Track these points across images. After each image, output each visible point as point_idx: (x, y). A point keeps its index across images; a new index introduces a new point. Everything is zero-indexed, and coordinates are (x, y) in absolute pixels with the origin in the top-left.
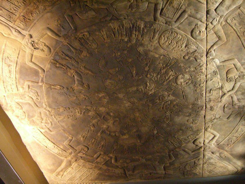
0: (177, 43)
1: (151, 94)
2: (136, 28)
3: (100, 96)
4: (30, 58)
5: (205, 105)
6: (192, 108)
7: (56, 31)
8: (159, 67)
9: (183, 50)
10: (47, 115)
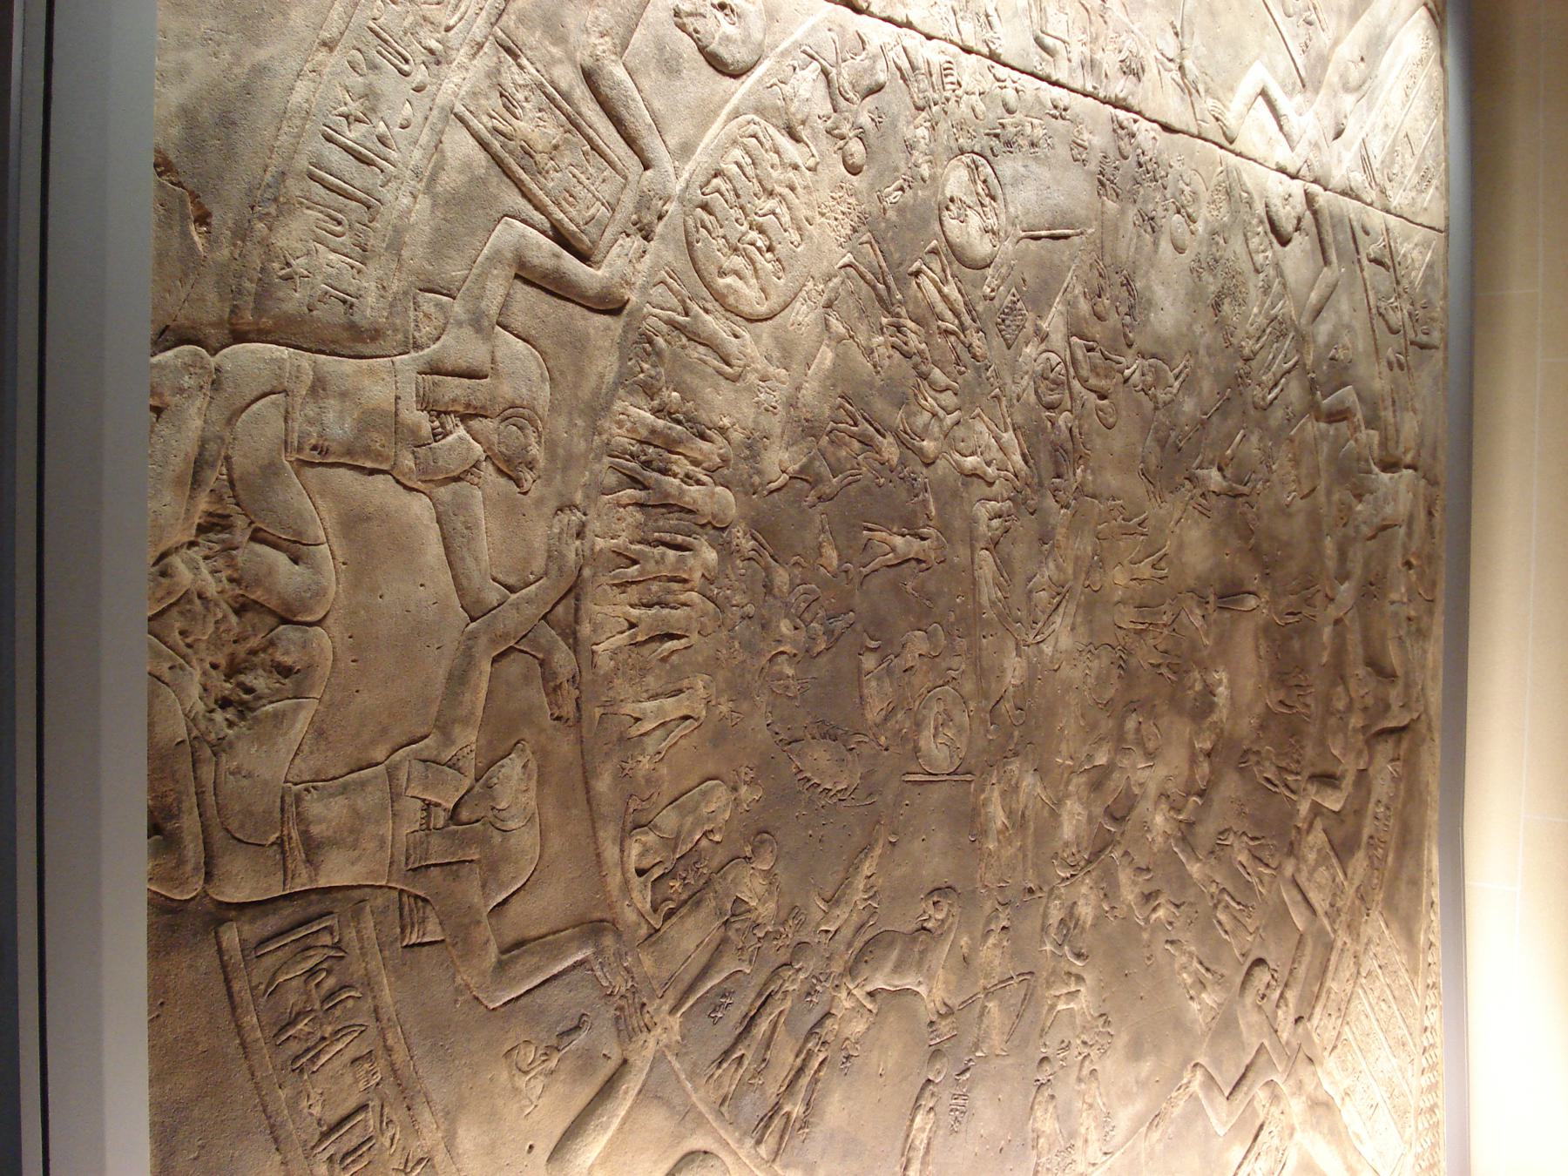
2: (647, 464)
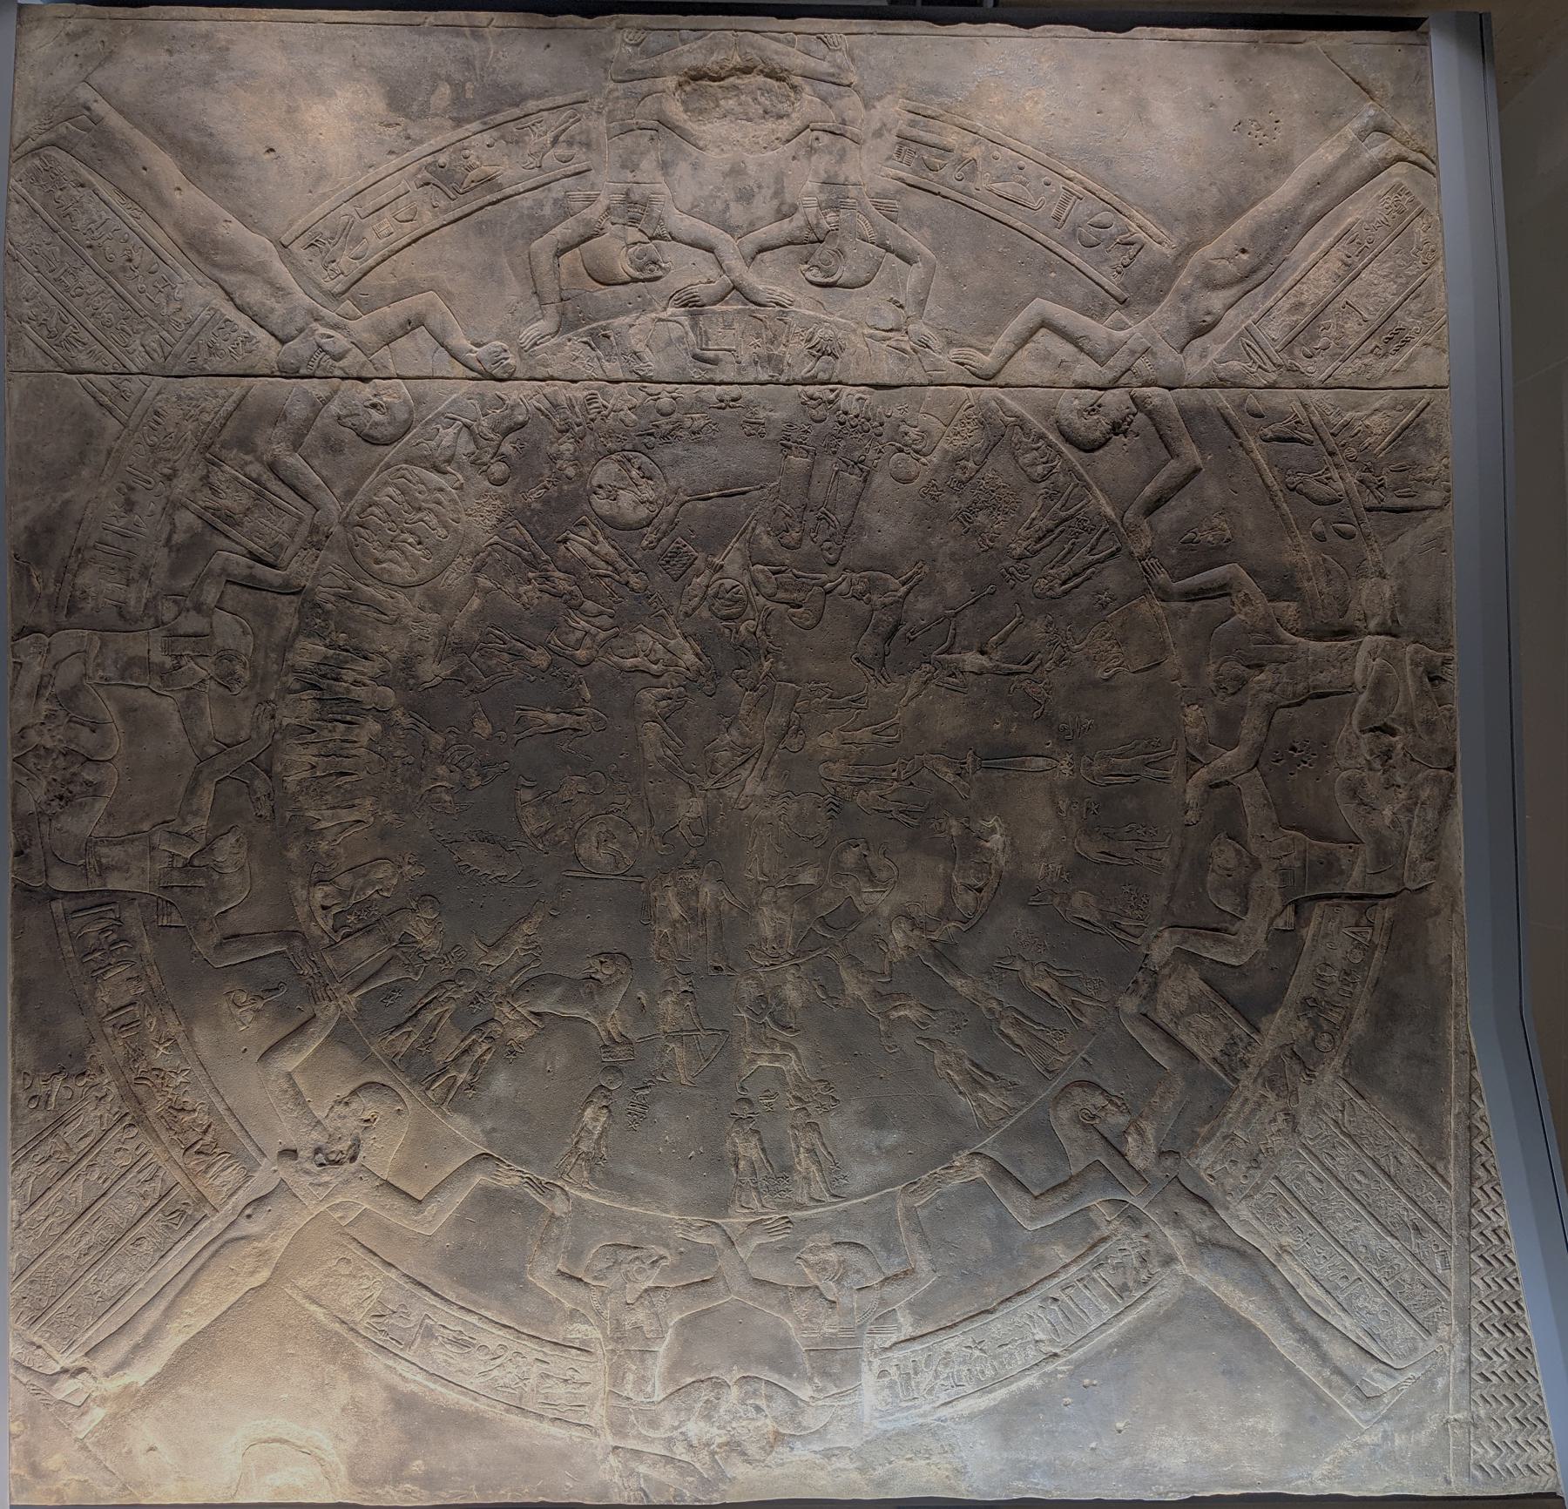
0: (420, 509)
1: (697, 655)
2: (324, 676)
3: (677, 911)
4: (398, 1202)
5: (800, 388)
6: (808, 451)
7: (283, 1030)
8: (536, 602)
9: (457, 485)
10: (784, 1249)
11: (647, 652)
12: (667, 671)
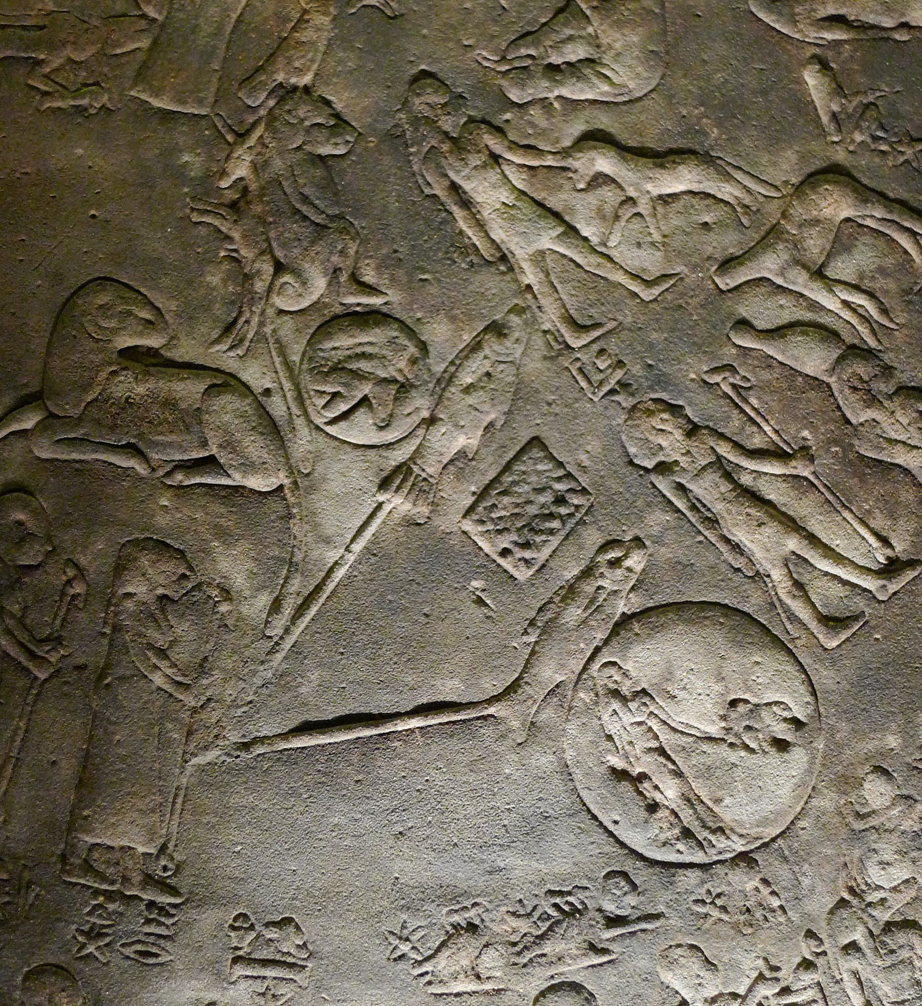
1: (466, 203)
11: (628, 212)
12: (565, 153)
